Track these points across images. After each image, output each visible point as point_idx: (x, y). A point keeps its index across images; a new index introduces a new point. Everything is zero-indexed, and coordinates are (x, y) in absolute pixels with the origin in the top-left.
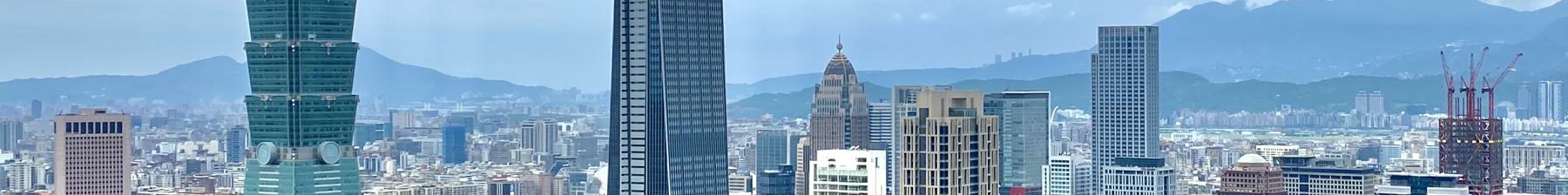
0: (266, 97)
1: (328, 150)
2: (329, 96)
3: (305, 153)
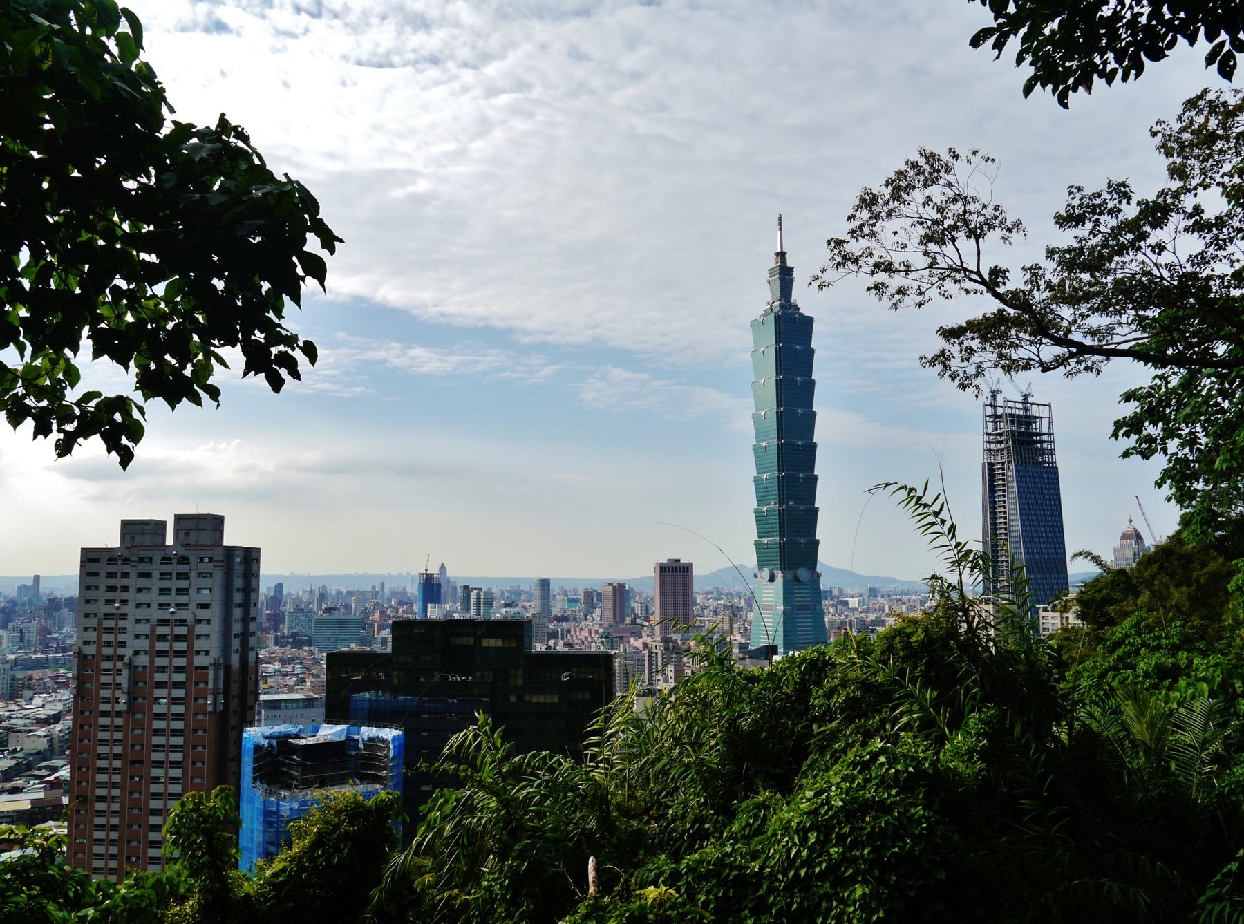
0: (766, 541)
1: (803, 573)
3: (790, 575)
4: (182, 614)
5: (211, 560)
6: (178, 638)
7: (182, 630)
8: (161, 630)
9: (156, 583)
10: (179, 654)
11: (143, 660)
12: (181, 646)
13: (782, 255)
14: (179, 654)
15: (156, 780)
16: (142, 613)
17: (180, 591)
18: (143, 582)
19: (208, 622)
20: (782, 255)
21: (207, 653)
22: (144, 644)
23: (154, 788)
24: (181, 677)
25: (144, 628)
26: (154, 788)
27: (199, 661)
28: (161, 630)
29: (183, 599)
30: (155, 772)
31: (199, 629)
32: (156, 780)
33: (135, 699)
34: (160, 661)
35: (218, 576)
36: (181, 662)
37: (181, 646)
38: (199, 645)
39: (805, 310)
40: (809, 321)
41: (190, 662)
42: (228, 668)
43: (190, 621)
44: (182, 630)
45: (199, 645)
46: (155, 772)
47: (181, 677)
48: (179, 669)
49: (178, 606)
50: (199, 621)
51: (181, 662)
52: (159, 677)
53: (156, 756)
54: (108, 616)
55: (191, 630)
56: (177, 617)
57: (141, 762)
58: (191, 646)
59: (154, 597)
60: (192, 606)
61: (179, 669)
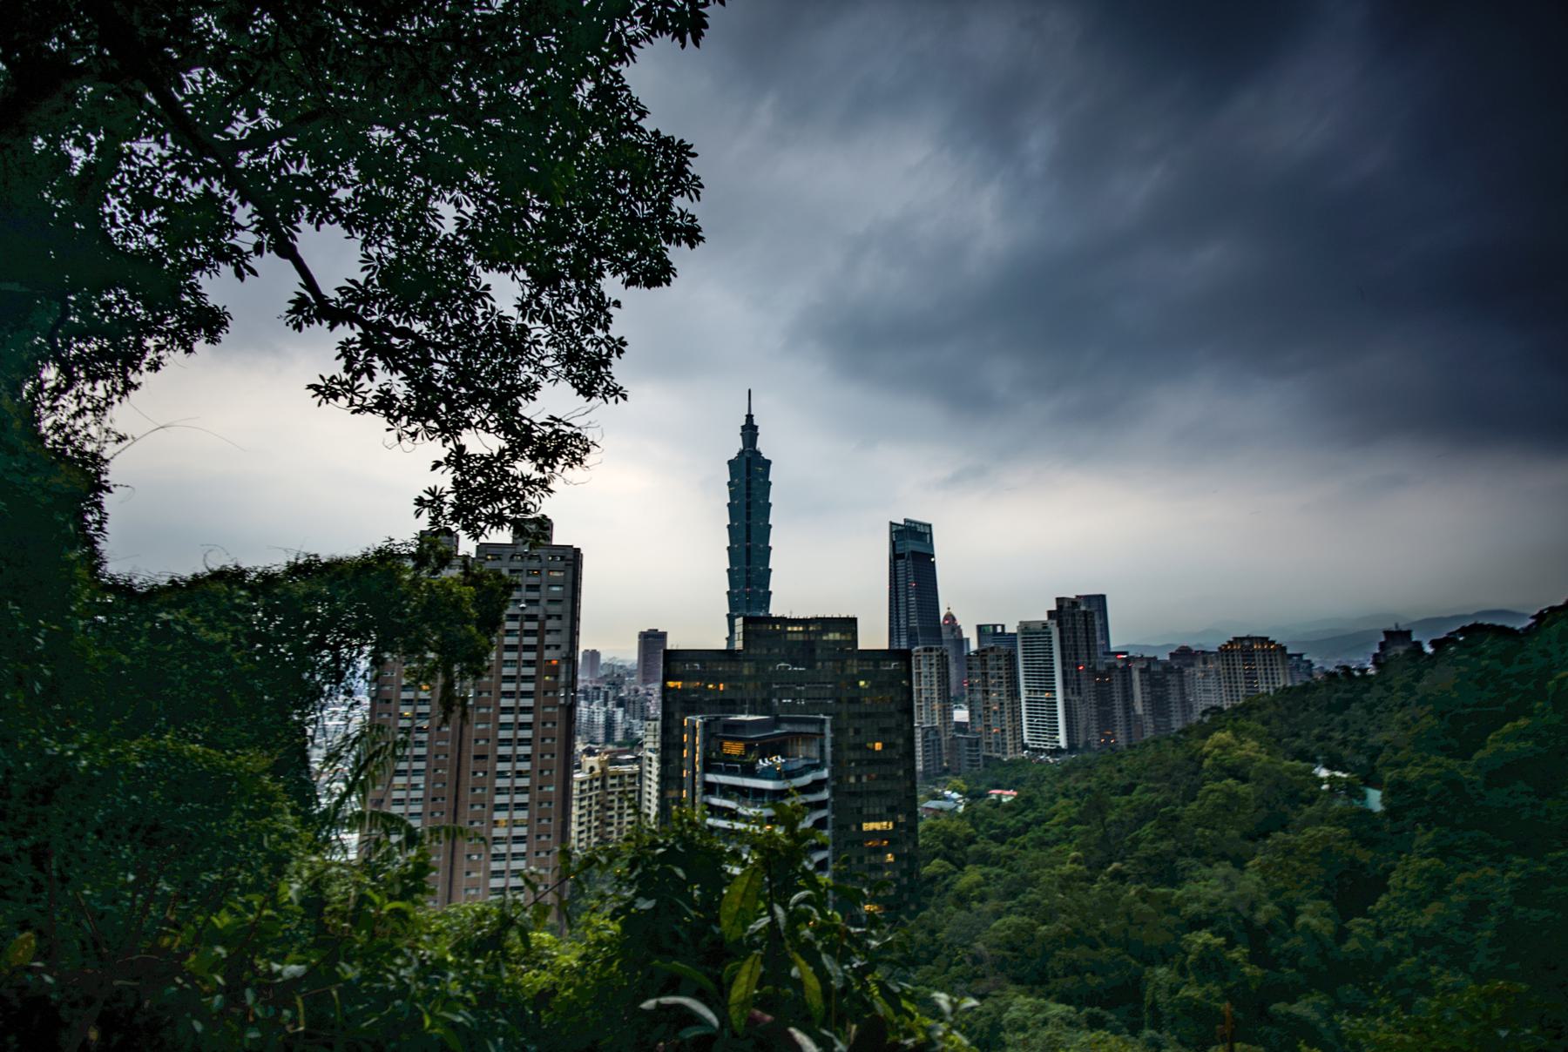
4: (533, 610)
5: (563, 558)
6: (528, 633)
7: (533, 625)
10: (528, 648)
12: (532, 640)
13: (750, 417)
14: (528, 648)
15: (502, 774)
17: (531, 588)
19: (559, 617)
20: (750, 417)
21: (557, 647)
23: (500, 783)
24: (531, 671)
26: (500, 783)
29: (533, 595)
30: (501, 766)
31: (550, 624)
32: (502, 774)
33: (480, 693)
36: (531, 656)
37: (532, 640)
39: (766, 456)
40: (769, 462)
41: (540, 656)
43: (541, 616)
44: (533, 625)
45: (549, 639)
46: (501, 766)
47: (531, 671)
48: (529, 663)
49: (527, 601)
50: (549, 617)
51: (531, 656)
53: (503, 750)
55: (542, 625)
56: (527, 612)
57: (484, 757)
58: (541, 641)
60: (543, 602)
61: (529, 663)
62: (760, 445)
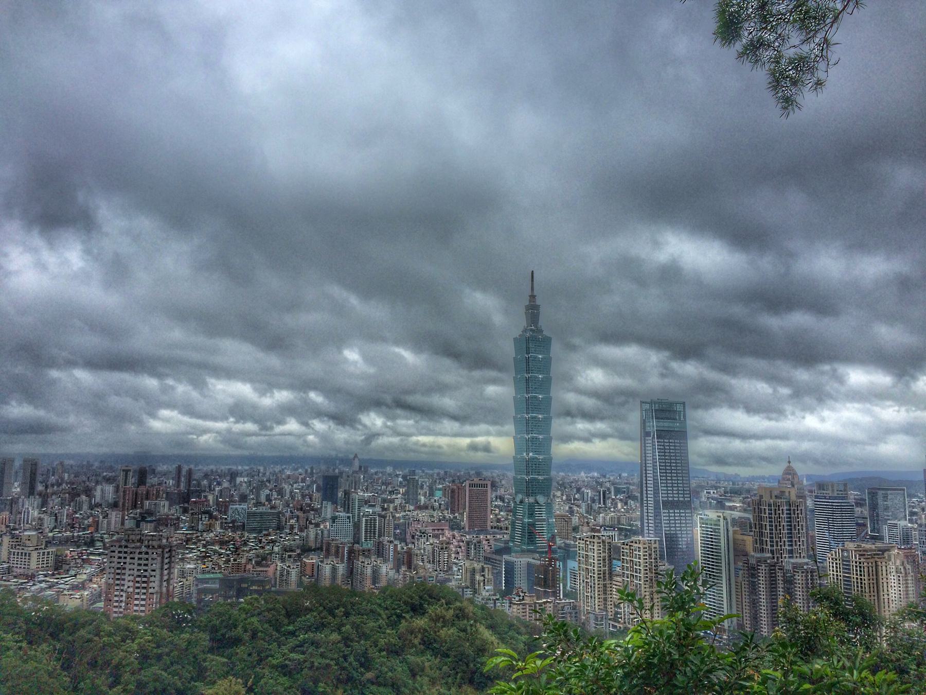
2: (540, 477)
3: (531, 500)
8: (138, 579)
9: (136, 561)
11: (131, 590)
12: (145, 585)
13: (533, 297)
16: (131, 572)
18: (132, 561)
20: (533, 297)
22: (131, 584)
24: (144, 597)
25: (131, 578)
27: (151, 591)
28: (138, 579)
31: (152, 579)
34: (137, 591)
35: (159, 559)
36: (145, 591)
38: (151, 585)
42: (161, 593)
52: (136, 596)
54: (118, 568)
59: (136, 567)
62: (542, 322)
